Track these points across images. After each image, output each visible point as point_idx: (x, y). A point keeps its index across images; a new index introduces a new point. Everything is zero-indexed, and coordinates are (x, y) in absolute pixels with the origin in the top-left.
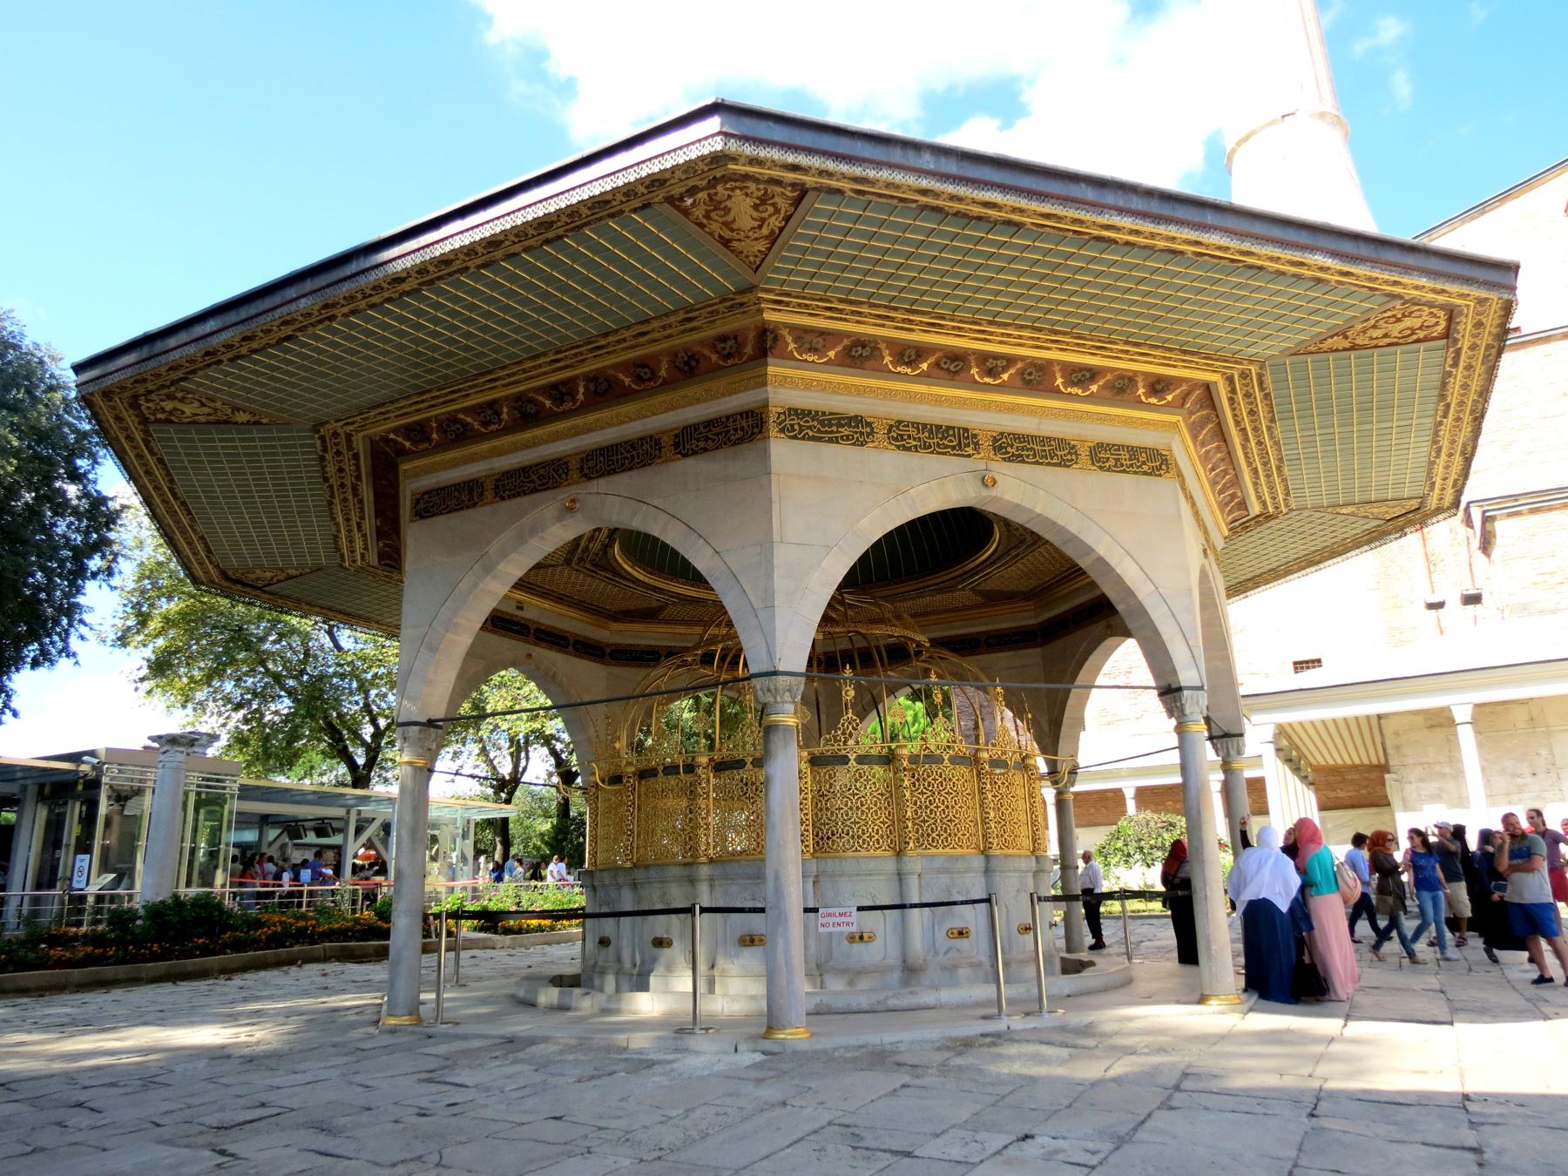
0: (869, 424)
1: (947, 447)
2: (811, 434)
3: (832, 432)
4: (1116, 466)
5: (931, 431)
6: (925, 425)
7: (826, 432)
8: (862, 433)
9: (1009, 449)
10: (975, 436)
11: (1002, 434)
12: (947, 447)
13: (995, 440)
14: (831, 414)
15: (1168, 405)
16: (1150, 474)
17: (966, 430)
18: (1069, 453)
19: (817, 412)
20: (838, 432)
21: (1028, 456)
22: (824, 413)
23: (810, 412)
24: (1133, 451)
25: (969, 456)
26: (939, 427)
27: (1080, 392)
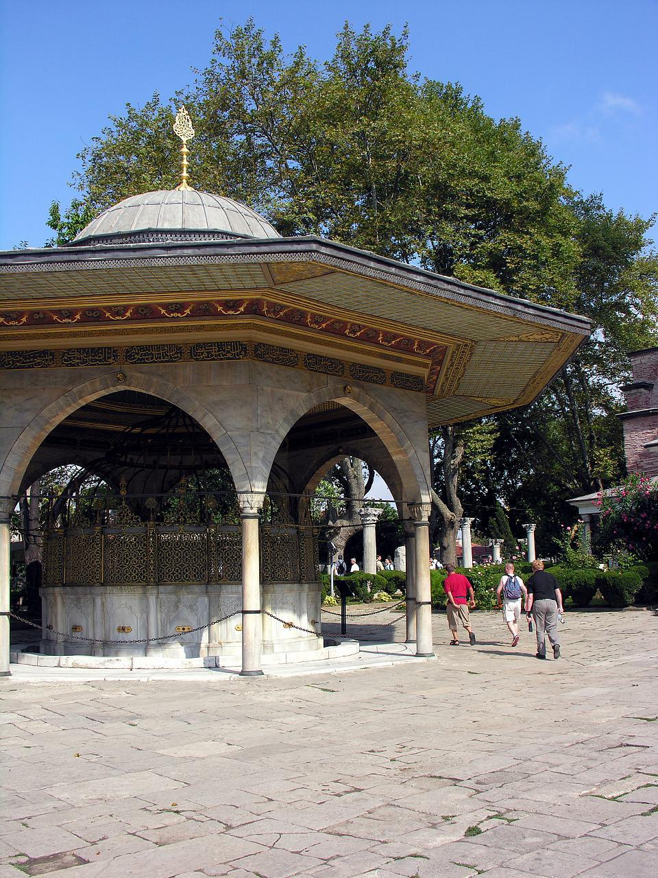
0: (52, 354)
1: (97, 360)
2: (18, 364)
3: (31, 362)
6: (84, 349)
7: (28, 362)
8: (47, 360)
10: (114, 351)
11: (132, 347)
12: (97, 360)
13: (128, 352)
14: (30, 351)
15: (242, 313)
16: (232, 359)
17: (109, 348)
18: (176, 353)
19: (23, 352)
20: (34, 361)
21: (147, 359)
23: (19, 352)
24: (220, 345)
25: (110, 364)
27: (179, 315)
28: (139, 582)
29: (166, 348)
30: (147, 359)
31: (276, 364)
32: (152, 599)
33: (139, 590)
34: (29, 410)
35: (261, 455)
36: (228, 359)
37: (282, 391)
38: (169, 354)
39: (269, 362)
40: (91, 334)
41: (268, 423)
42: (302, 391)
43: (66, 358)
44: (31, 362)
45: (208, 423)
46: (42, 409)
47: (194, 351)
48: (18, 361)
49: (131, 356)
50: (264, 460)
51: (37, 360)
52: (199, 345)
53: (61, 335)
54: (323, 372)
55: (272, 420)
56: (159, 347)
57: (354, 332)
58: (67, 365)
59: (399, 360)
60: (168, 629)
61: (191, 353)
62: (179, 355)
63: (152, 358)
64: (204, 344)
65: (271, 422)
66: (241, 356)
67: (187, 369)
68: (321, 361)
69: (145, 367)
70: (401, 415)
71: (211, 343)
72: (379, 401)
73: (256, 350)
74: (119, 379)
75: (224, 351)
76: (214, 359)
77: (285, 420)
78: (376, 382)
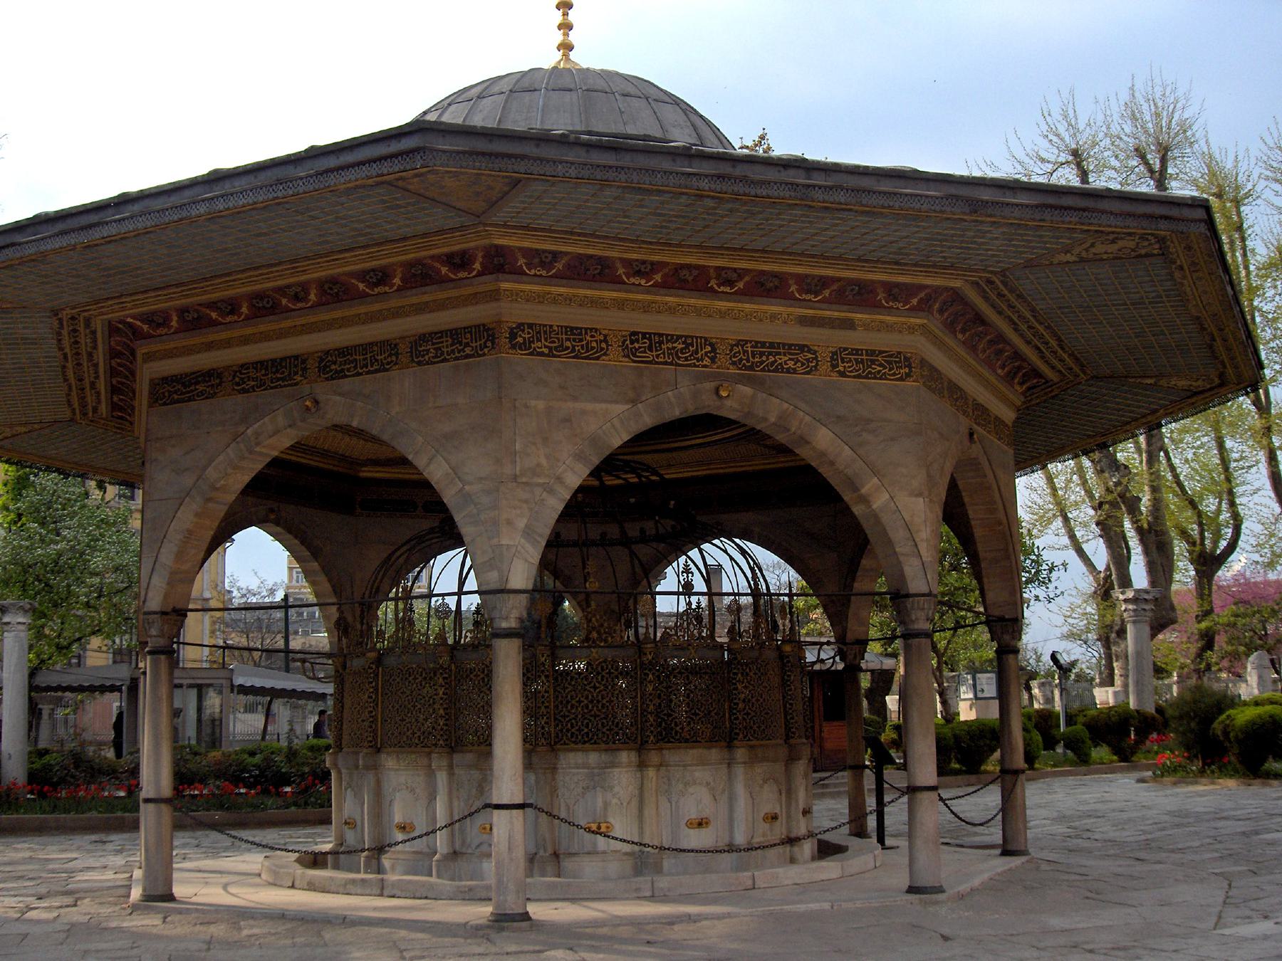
0: (220, 376)
1: (278, 379)
2: (176, 397)
3: (192, 391)
4: (436, 357)
5: (266, 369)
7: (189, 392)
9: (333, 367)
12: (278, 379)
15: (479, 274)
17: (296, 357)
18: (390, 355)
21: (348, 370)
22: (186, 375)
25: (296, 384)
26: (274, 361)
27: (387, 289)
28: (565, 744)
29: (375, 348)
30: (348, 370)
31: (559, 356)
32: (442, 778)
33: (714, 754)
34: (186, 470)
35: (521, 523)
36: (467, 356)
37: (570, 404)
38: (379, 358)
39: (542, 354)
40: (266, 337)
41: (539, 465)
42: (616, 402)
43: (237, 379)
44: (192, 391)
45: (436, 471)
46: (205, 468)
47: (416, 349)
48: (175, 392)
49: (325, 366)
50: (528, 532)
51: (200, 388)
52: (423, 338)
53: (228, 344)
54: (666, 363)
55: (547, 457)
56: (366, 347)
57: (730, 283)
58: (239, 392)
59: (849, 325)
60: (468, 829)
61: (411, 352)
62: (394, 358)
63: (355, 367)
64: (430, 334)
65: (544, 462)
66: (486, 350)
67: (403, 382)
68: (661, 343)
69: (346, 384)
70: (858, 429)
71: (441, 332)
72: (802, 405)
73: (513, 335)
74: (308, 409)
75: (460, 343)
76: (447, 360)
77: (579, 457)
78: (795, 371)
